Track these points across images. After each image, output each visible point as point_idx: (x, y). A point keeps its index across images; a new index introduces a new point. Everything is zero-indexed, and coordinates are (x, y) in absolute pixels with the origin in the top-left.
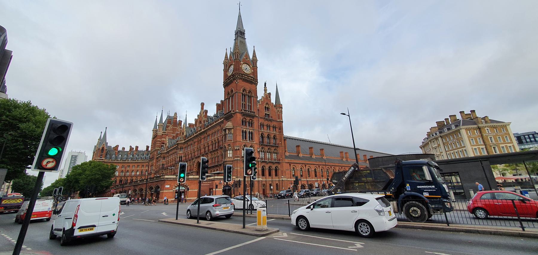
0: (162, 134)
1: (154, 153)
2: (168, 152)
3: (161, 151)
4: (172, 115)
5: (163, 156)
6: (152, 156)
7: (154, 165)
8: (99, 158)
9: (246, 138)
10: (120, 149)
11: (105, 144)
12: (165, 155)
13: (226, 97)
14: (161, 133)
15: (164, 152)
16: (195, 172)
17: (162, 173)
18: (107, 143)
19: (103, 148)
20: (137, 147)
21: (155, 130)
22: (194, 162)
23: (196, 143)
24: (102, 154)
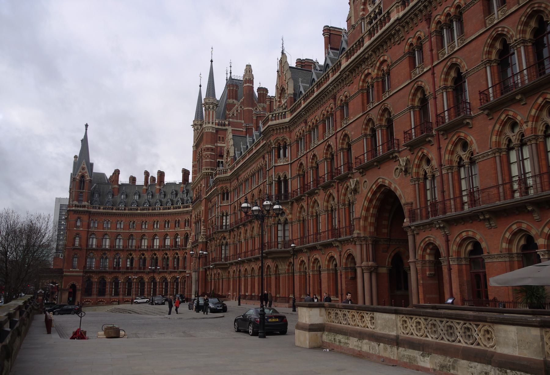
0: (217, 130)
1: (199, 185)
2: (236, 175)
4: (239, 74)
5: (222, 188)
6: (196, 195)
7: (202, 219)
8: (76, 203)
10: (123, 179)
11: (85, 166)
12: (228, 185)
14: (214, 126)
16: (365, 239)
17: (224, 242)
18: (92, 165)
19: (83, 176)
20: (161, 174)
21: (200, 123)
22: (355, 191)
23: (355, 104)
24: (81, 193)
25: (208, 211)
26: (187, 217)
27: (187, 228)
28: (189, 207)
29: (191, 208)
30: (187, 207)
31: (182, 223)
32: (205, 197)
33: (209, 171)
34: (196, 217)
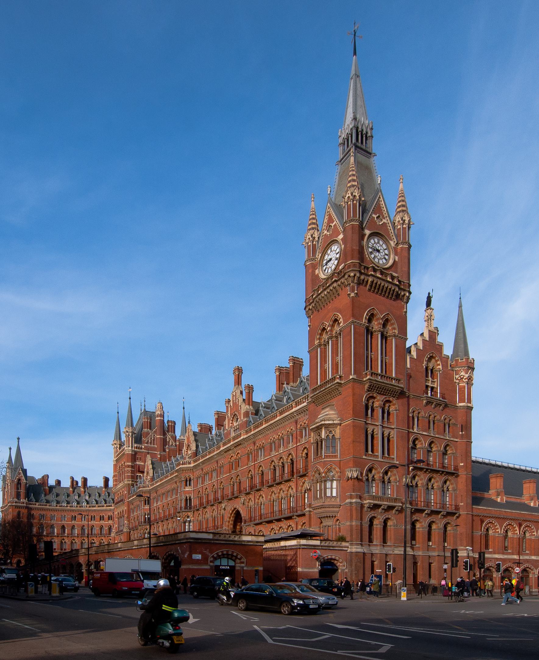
3: (140, 488)
9: (375, 451)
13: (317, 342)
15: (145, 489)
25: (129, 511)
26: (110, 514)
27: (110, 522)
28: (112, 506)
29: (113, 507)
30: (110, 506)
31: (106, 517)
32: (128, 500)
33: (131, 482)
34: (118, 514)
